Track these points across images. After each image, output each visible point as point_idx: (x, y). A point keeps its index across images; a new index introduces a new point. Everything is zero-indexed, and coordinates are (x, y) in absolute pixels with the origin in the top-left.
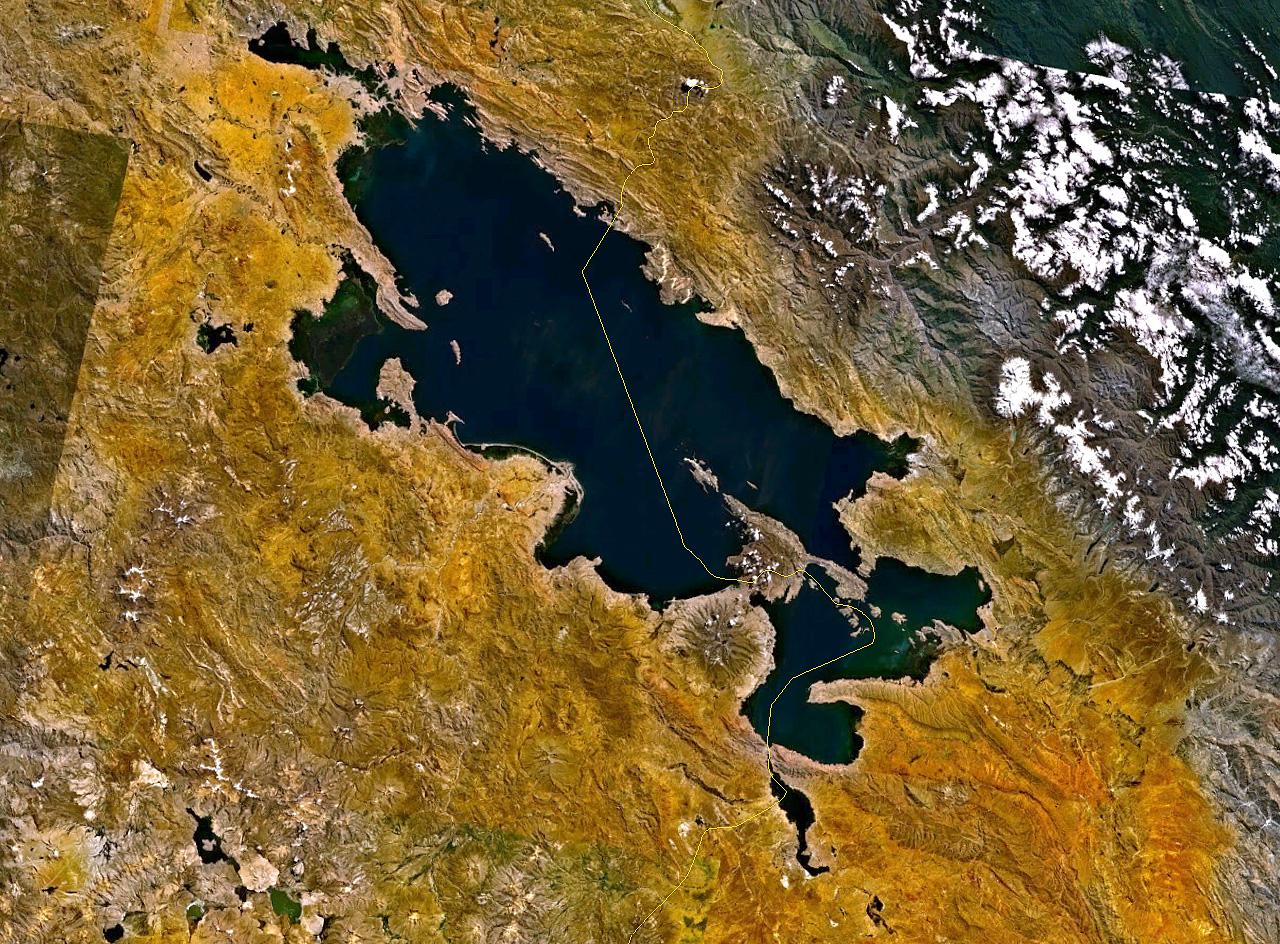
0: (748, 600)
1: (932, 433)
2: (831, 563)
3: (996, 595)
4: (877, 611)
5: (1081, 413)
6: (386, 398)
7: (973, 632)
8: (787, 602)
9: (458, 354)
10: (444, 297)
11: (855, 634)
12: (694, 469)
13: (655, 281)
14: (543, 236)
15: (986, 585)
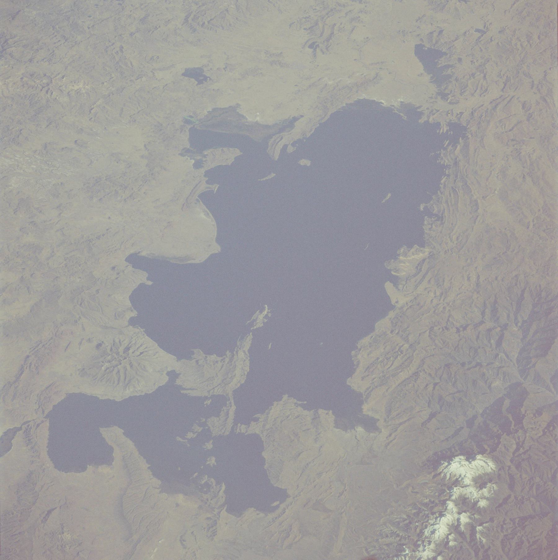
0: (169, 369)
1: (390, 435)
2: (234, 408)
3: (271, 516)
4: (209, 446)
5: (476, 516)
6: (207, 155)
7: (229, 511)
8: (182, 392)
9: (267, 178)
10: (305, 162)
11: (179, 439)
12: (261, 312)
13: (399, 255)
14: (389, 195)
15: (278, 507)
